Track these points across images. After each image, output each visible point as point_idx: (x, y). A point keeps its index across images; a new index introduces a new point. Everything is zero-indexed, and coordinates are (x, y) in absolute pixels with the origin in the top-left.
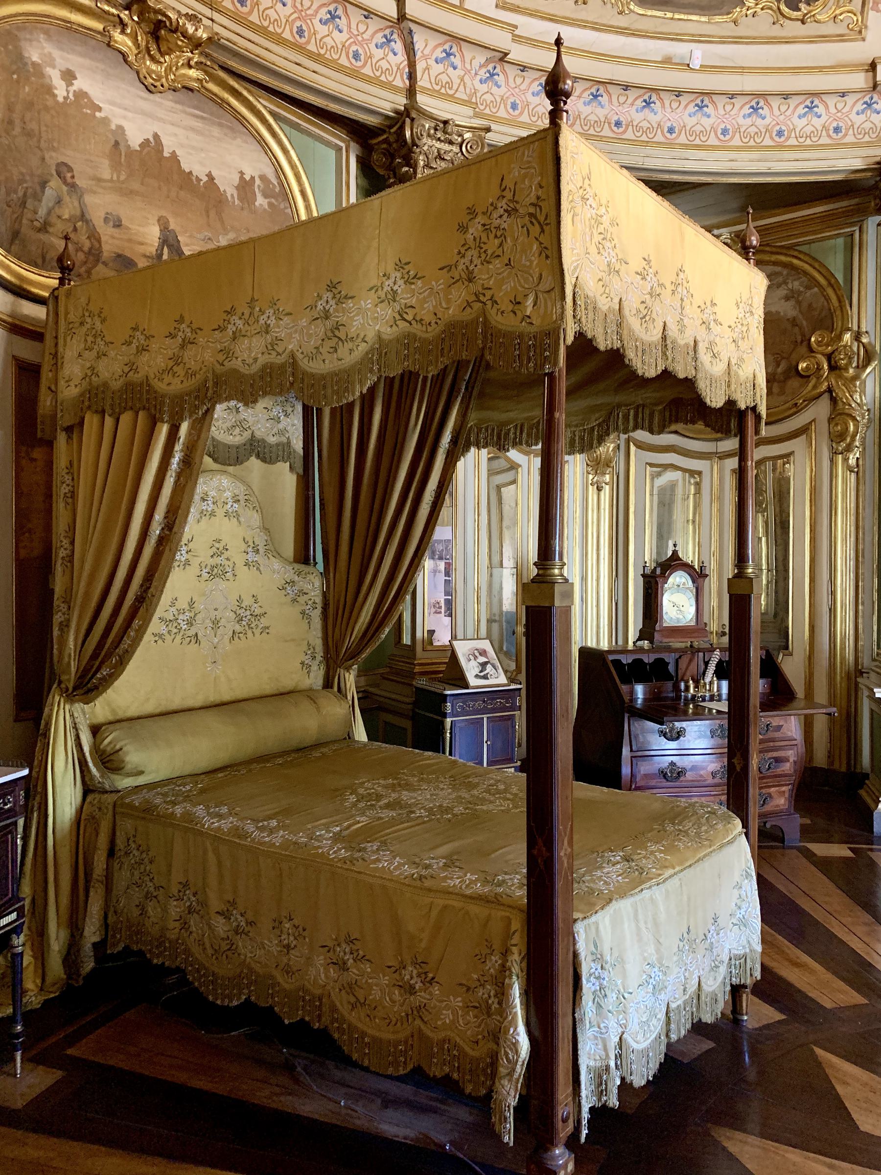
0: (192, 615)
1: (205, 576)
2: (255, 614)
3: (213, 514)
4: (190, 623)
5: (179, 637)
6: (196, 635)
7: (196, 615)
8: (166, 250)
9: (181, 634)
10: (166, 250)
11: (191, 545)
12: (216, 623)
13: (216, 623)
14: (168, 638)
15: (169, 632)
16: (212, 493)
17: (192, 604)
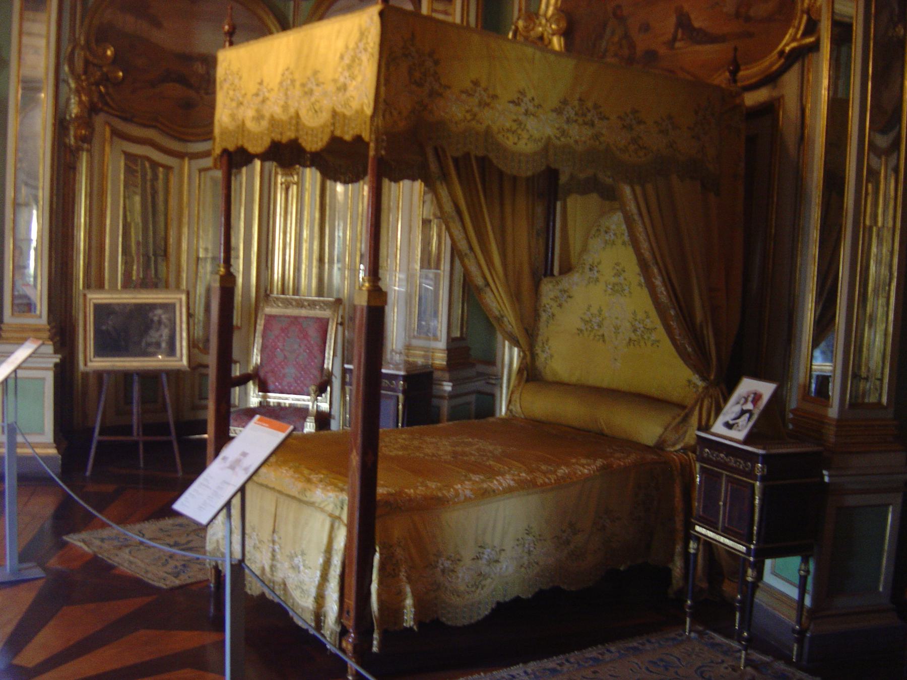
0: (601, 319)
1: (610, 291)
2: (647, 327)
3: (613, 243)
4: (600, 326)
5: (592, 334)
6: (603, 335)
7: (603, 319)
8: (680, 31)
9: (594, 331)
10: (680, 31)
11: (600, 267)
12: (617, 328)
13: (617, 328)
14: (586, 333)
15: (587, 329)
16: (613, 227)
17: (600, 311)
